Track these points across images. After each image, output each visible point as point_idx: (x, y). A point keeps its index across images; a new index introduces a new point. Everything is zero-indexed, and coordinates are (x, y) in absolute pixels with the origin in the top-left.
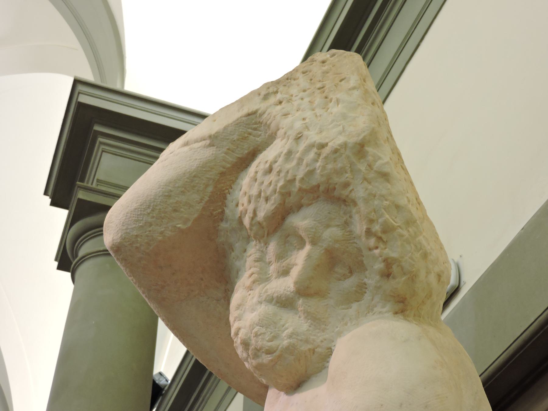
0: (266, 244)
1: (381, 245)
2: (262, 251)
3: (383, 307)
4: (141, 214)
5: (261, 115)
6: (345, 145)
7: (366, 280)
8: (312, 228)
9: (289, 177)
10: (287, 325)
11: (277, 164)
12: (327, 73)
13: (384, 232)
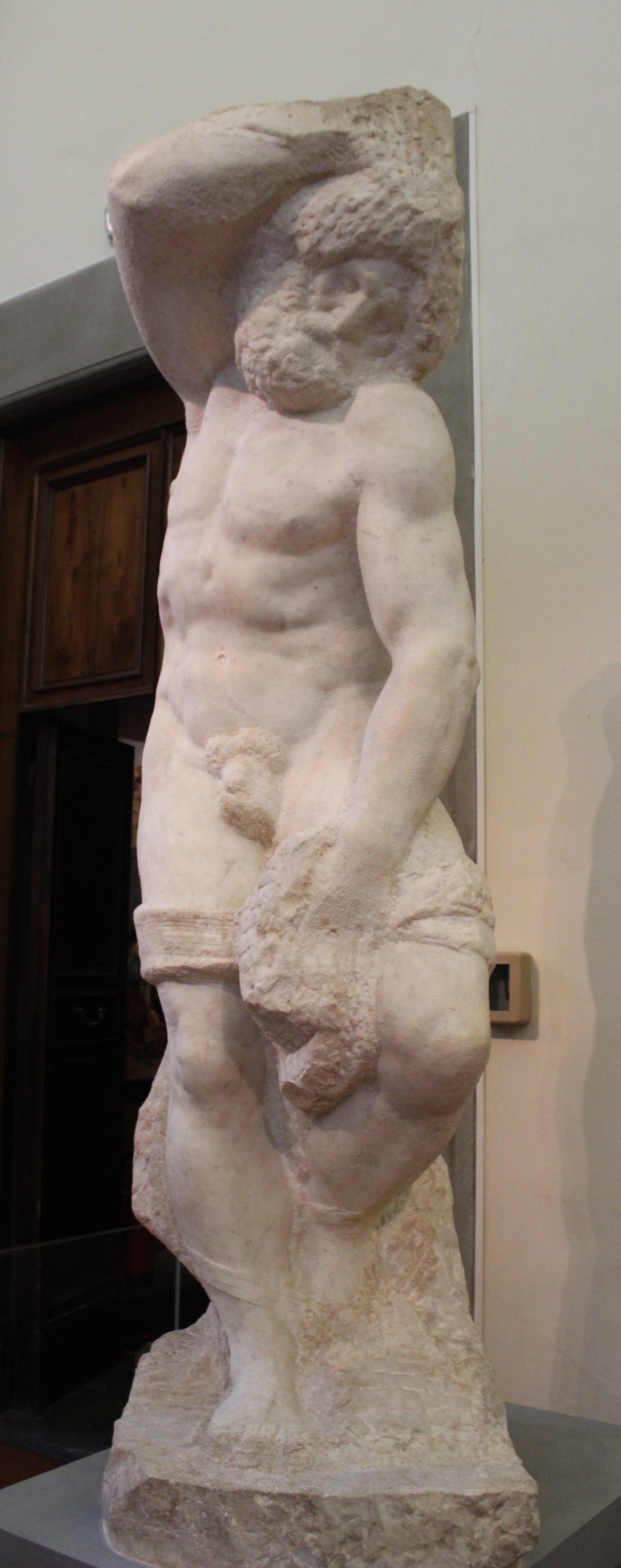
2: (307, 278)
3: (406, 370)
6: (438, 221)
7: (398, 342)
9: (375, 227)
10: (320, 360)
11: (365, 208)
13: (439, 311)
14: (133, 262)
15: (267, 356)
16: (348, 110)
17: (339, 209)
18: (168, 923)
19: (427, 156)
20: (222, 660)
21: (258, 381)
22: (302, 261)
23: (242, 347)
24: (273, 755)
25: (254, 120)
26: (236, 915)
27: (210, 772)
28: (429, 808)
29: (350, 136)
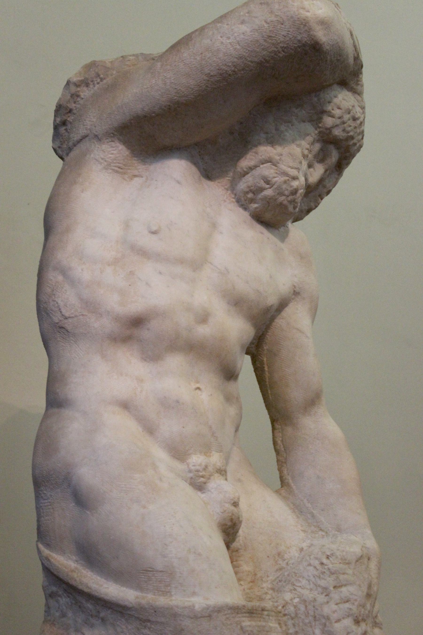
14: (260, 64)
18: (245, 615)
26: (280, 608)
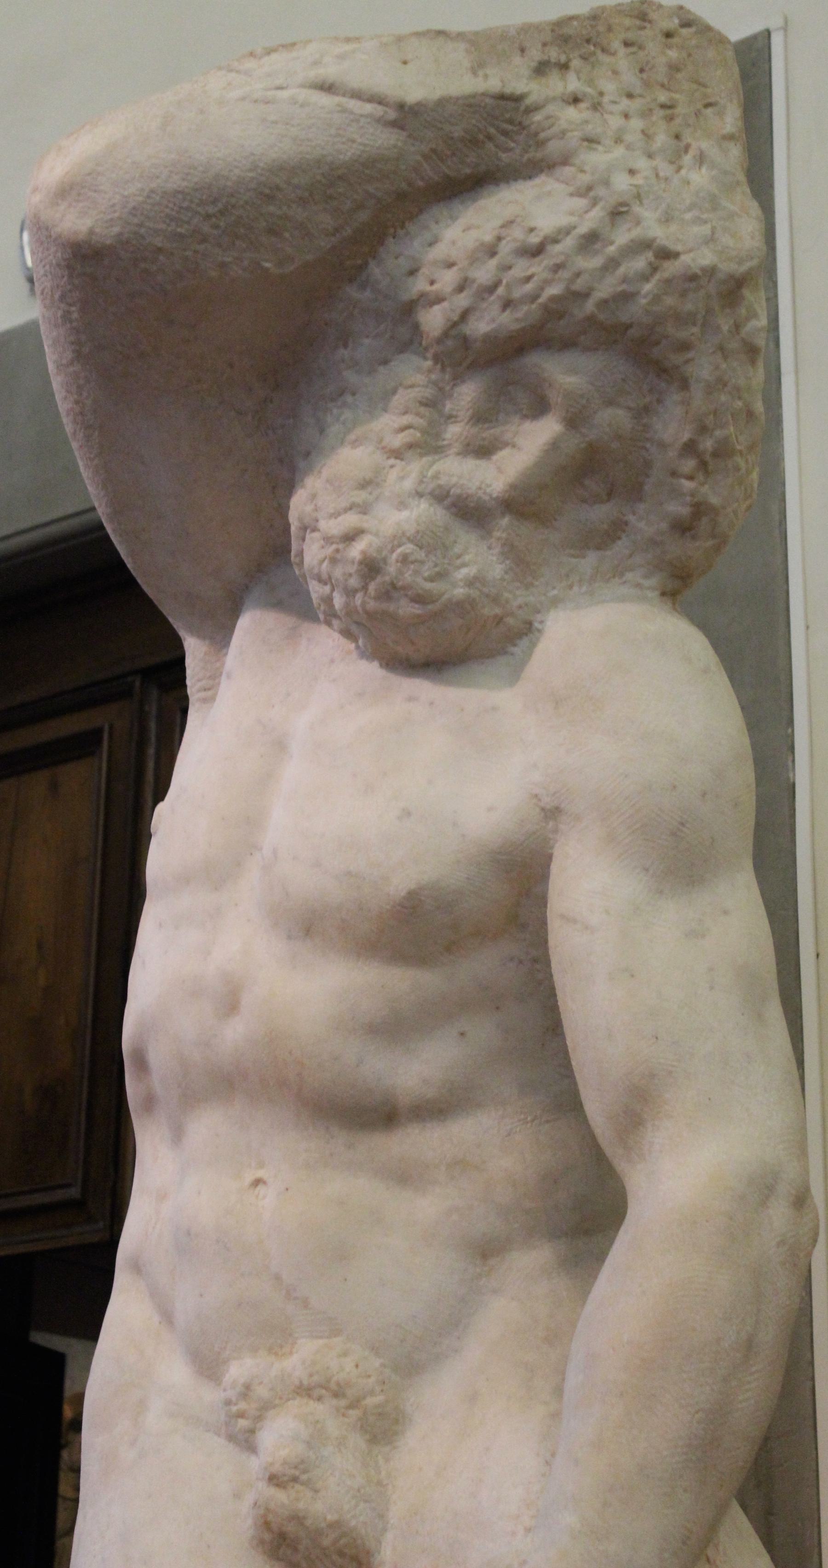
0: (454, 379)
1: (701, 477)
2: (441, 389)
3: (646, 577)
4: (188, 209)
5: (529, 110)
6: (710, 272)
7: (631, 518)
8: (582, 396)
9: (579, 285)
10: (467, 558)
11: (558, 248)
12: (678, 70)
13: (716, 454)
14: (78, 356)
15: (356, 551)
16: (522, 50)
17: (505, 248)
19: (687, 138)
20: (261, 1189)
21: (338, 601)
22: (429, 355)
23: (304, 528)
24: (370, 1401)
25: (330, 71)
27: (231, 1438)
28: (713, 1527)
29: (528, 101)
